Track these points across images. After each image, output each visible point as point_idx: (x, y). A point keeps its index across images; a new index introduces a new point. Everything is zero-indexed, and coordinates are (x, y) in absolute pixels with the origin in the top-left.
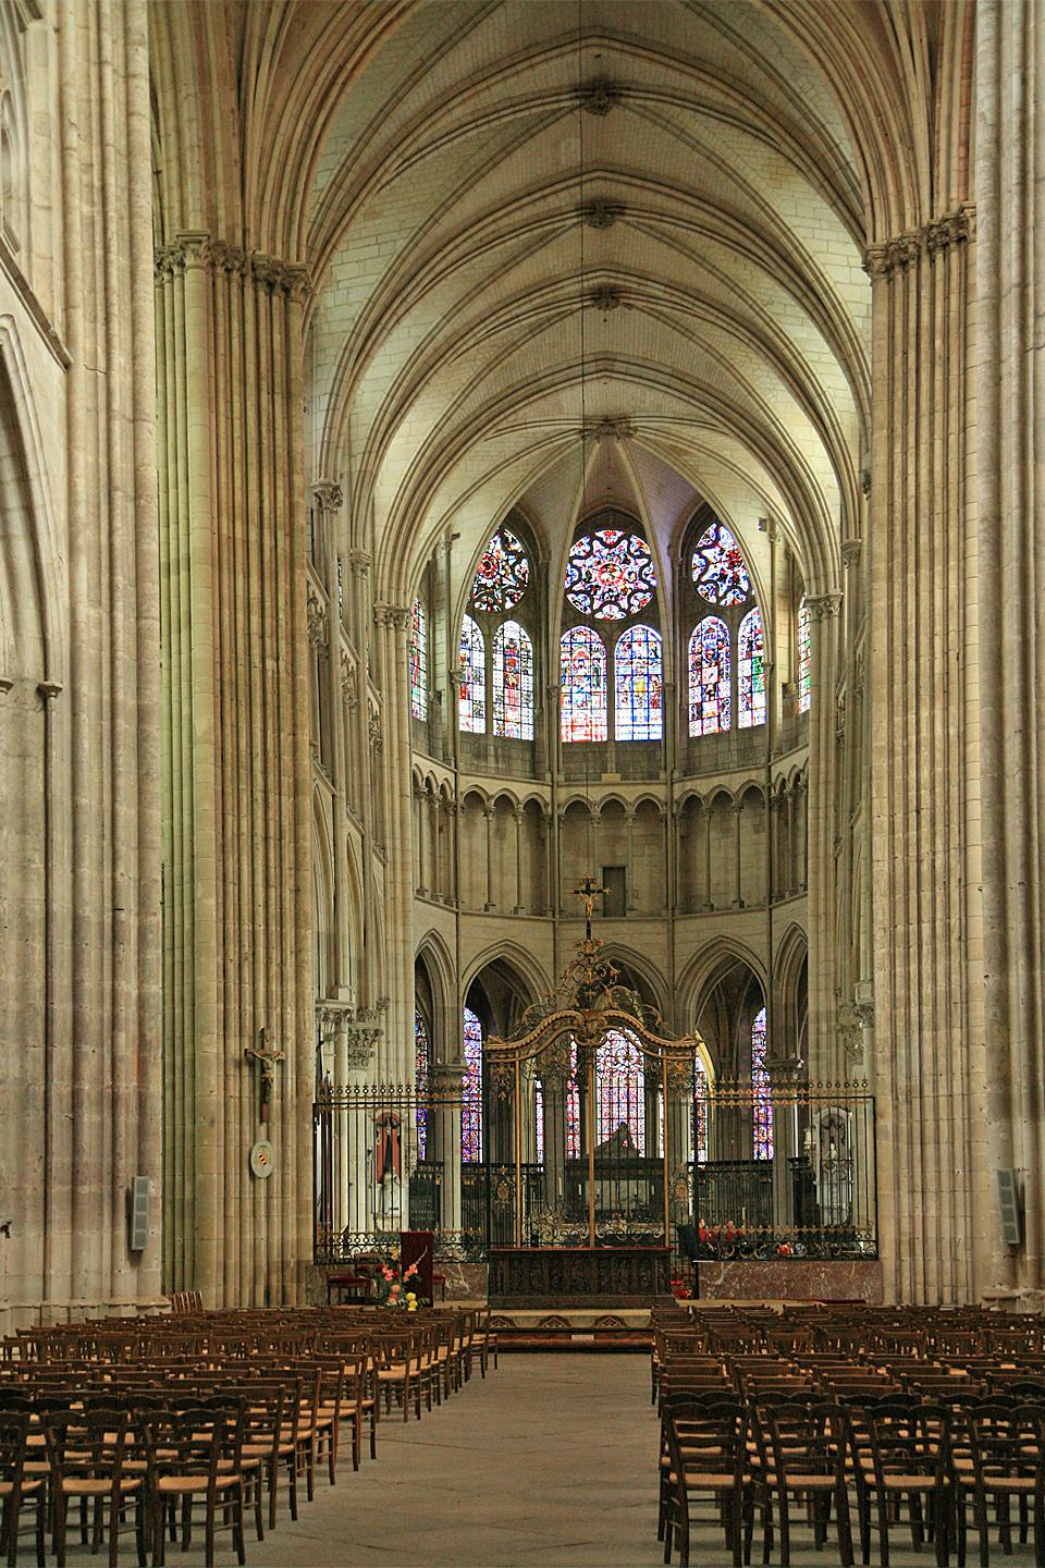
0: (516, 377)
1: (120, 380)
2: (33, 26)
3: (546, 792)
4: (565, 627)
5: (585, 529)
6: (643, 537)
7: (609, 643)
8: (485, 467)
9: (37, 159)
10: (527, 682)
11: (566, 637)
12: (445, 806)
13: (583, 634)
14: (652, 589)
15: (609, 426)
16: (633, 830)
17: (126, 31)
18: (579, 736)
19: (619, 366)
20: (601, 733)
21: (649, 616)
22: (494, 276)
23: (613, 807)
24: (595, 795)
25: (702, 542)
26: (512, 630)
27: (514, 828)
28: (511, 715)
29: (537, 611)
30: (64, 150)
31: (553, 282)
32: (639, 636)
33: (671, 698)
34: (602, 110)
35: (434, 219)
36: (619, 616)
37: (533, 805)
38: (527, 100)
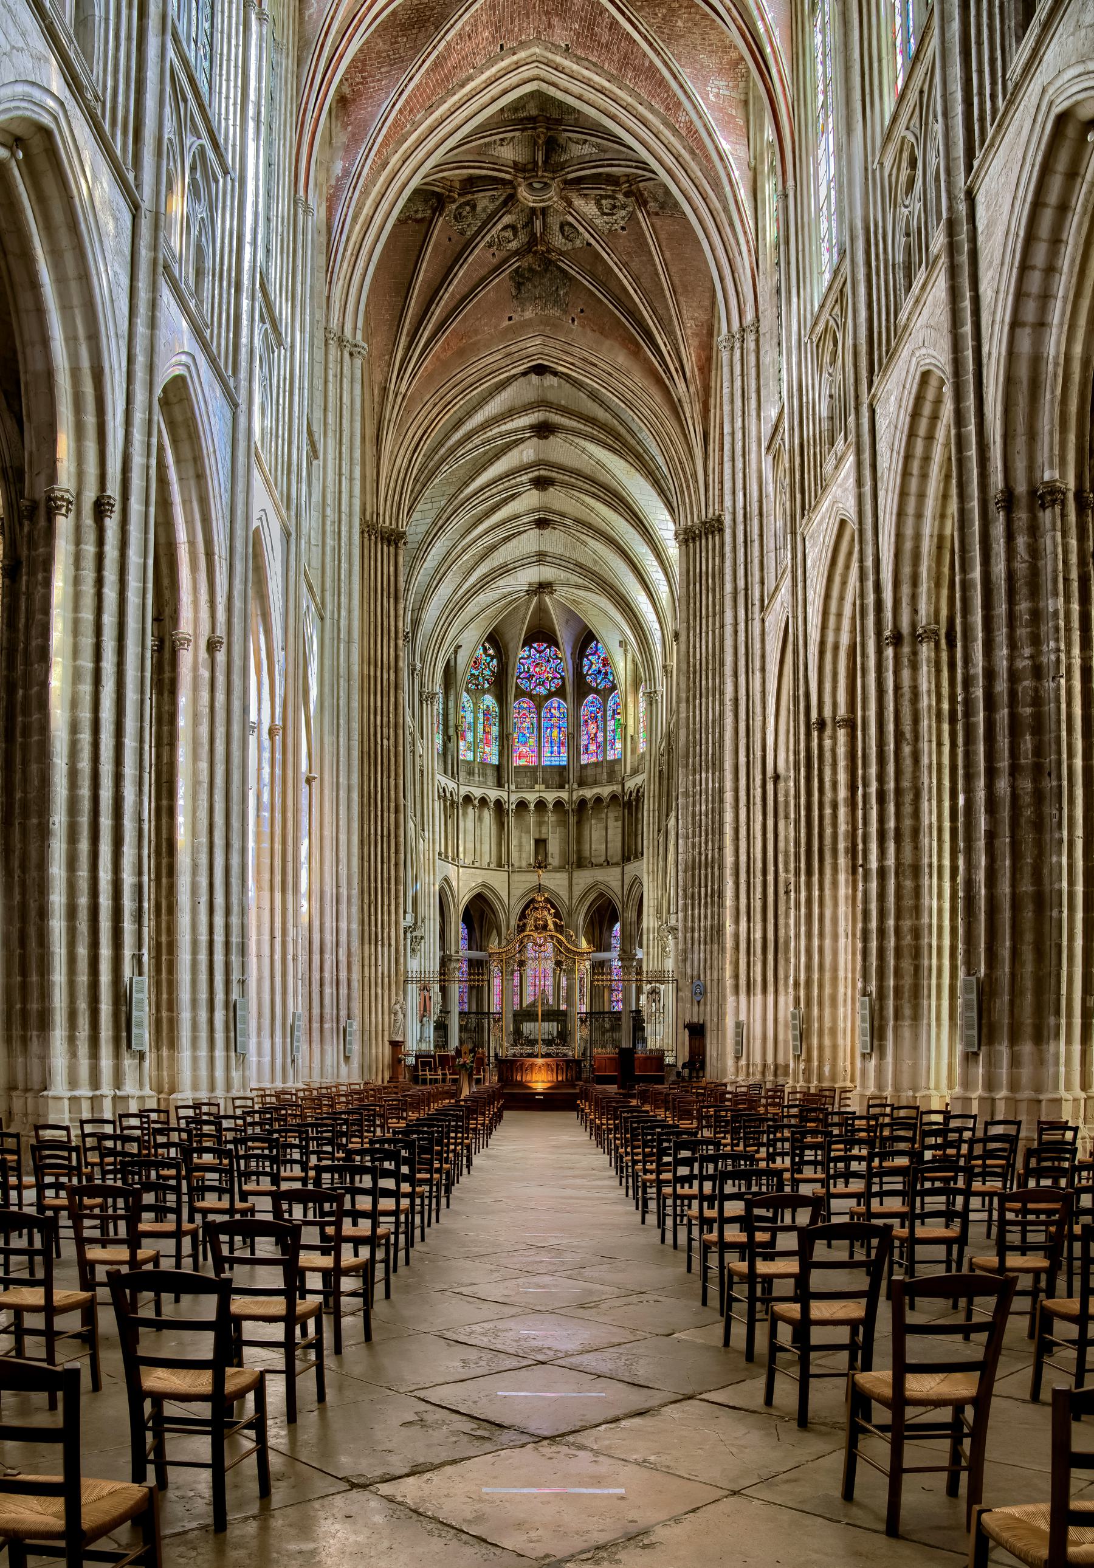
0: (496, 564)
1: (343, 623)
2: (315, 462)
3: (505, 795)
4: (516, 698)
5: (528, 642)
6: (557, 646)
7: (539, 708)
8: (476, 610)
9: (313, 523)
10: (495, 730)
11: (516, 704)
12: (453, 802)
13: (525, 703)
14: (562, 678)
15: (543, 587)
16: (551, 818)
17: (351, 459)
18: (523, 762)
19: (548, 559)
20: (533, 761)
21: (560, 692)
22: (488, 514)
23: (541, 805)
24: (531, 797)
25: (589, 651)
26: (489, 700)
27: (488, 815)
28: (487, 749)
29: (501, 689)
30: (324, 516)
31: (516, 517)
32: (555, 705)
33: (572, 739)
34: (546, 438)
35: (460, 490)
36: (545, 692)
37: (498, 803)
38: (509, 433)
